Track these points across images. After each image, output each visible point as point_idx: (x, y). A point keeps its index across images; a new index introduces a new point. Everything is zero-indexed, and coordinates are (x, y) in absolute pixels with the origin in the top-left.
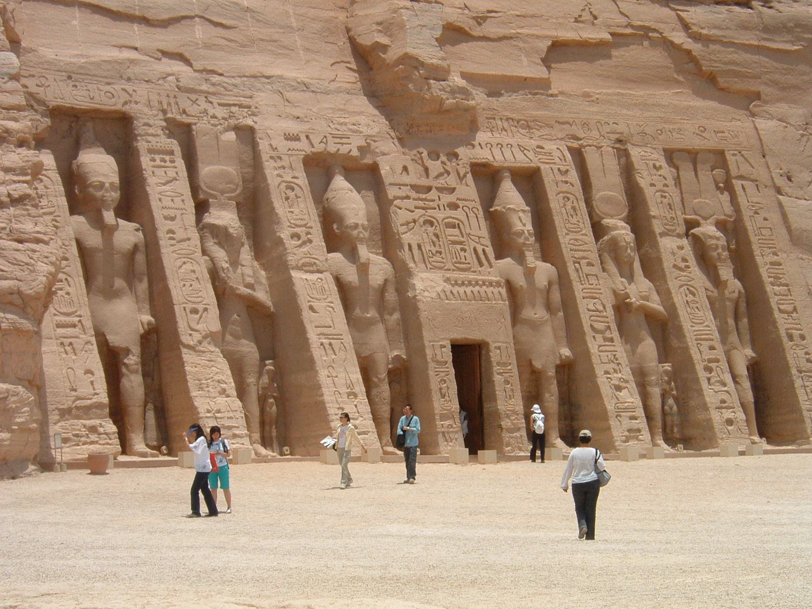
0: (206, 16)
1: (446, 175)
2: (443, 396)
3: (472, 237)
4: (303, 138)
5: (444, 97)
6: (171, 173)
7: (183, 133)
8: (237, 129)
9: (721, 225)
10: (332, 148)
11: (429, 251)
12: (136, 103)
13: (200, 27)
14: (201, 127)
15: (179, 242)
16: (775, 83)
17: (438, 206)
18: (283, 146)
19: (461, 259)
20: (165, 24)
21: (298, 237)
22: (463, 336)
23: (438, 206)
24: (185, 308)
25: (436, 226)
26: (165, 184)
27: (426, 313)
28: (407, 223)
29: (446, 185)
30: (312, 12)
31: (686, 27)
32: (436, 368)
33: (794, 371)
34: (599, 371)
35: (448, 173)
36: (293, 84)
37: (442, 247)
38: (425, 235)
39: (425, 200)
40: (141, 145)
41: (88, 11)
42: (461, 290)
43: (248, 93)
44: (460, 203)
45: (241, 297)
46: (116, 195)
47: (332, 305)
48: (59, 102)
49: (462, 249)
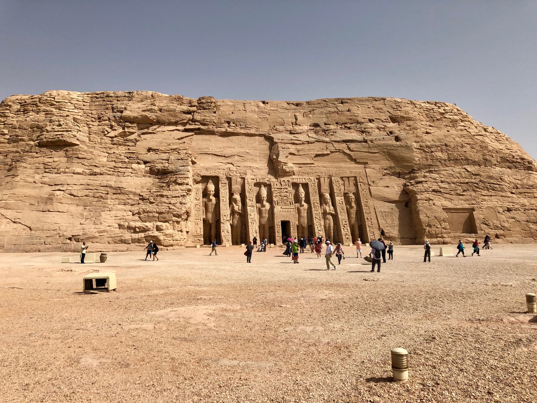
7: (229, 179)
8: (241, 178)
9: (353, 194)
10: (261, 181)
14: (233, 178)
16: (372, 160)
18: (250, 181)
30: (262, 152)
31: (349, 148)
33: (367, 227)
34: (316, 227)
40: (220, 182)
46: (214, 192)
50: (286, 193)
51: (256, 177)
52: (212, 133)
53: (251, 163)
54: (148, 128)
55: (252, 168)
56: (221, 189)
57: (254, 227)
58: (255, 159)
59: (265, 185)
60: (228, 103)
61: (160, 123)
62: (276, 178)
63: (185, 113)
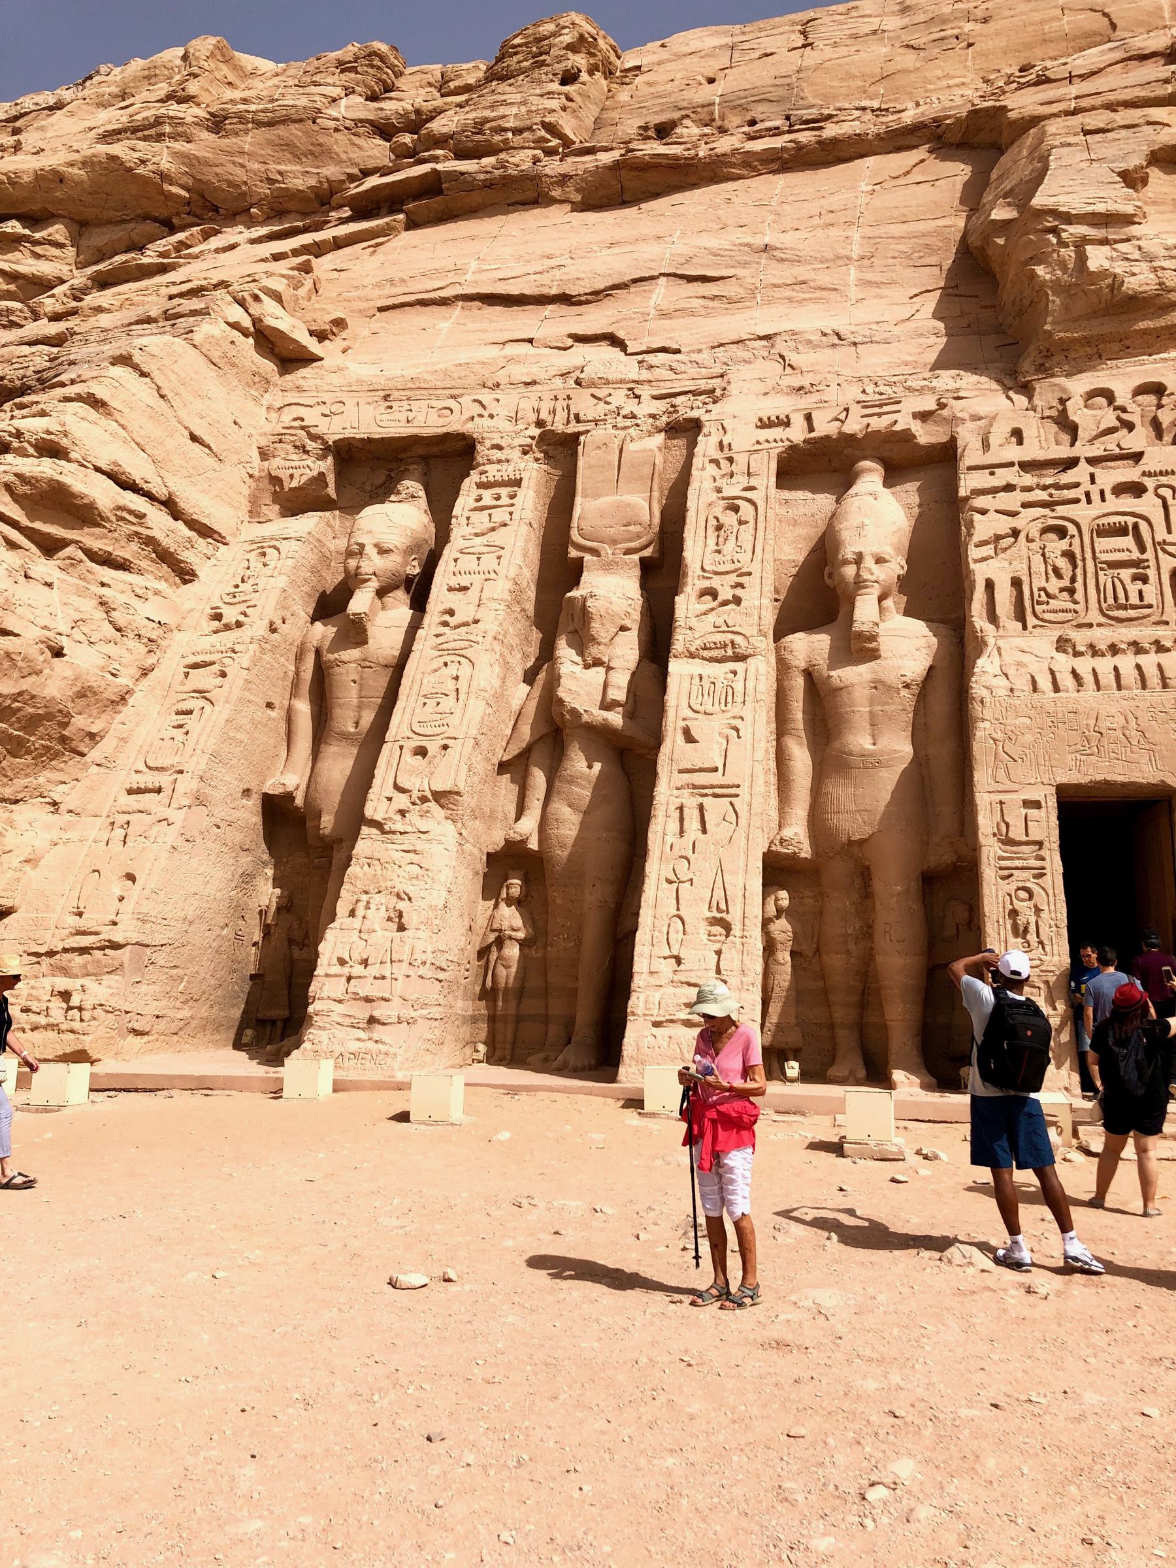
0: (679, 272)
1: (1125, 431)
2: (1021, 932)
3: (1170, 549)
4: (798, 421)
5: (1118, 271)
6: (500, 515)
7: (560, 448)
10: (854, 426)
11: (1039, 590)
12: (491, 416)
13: (663, 290)
15: (456, 627)
17: (1088, 494)
18: (743, 436)
19: (1127, 599)
20: (597, 296)
21: (713, 593)
22: (1100, 778)
23: (1088, 494)
24: (401, 748)
25: (1073, 536)
26: (477, 535)
27: (986, 724)
28: (998, 538)
29: (1117, 451)
32: (1001, 858)
35: (1130, 427)
36: (812, 338)
37: (1080, 579)
38: (1037, 560)
39: (1057, 487)
41: (478, 303)
42: (1104, 665)
43: (718, 370)
44: (1150, 483)
45: (590, 727)
47: (737, 723)
48: (348, 434)
49: (1135, 578)
50: (1127, 503)
51: (806, 402)
52: (524, 194)
53: (782, 309)
54: (141, 249)
55: (780, 346)
56: (459, 531)
57: (704, 870)
58: (824, 279)
59: (901, 459)
60: (695, 45)
61: (213, 206)
62: (1016, 382)
63: (384, 130)
